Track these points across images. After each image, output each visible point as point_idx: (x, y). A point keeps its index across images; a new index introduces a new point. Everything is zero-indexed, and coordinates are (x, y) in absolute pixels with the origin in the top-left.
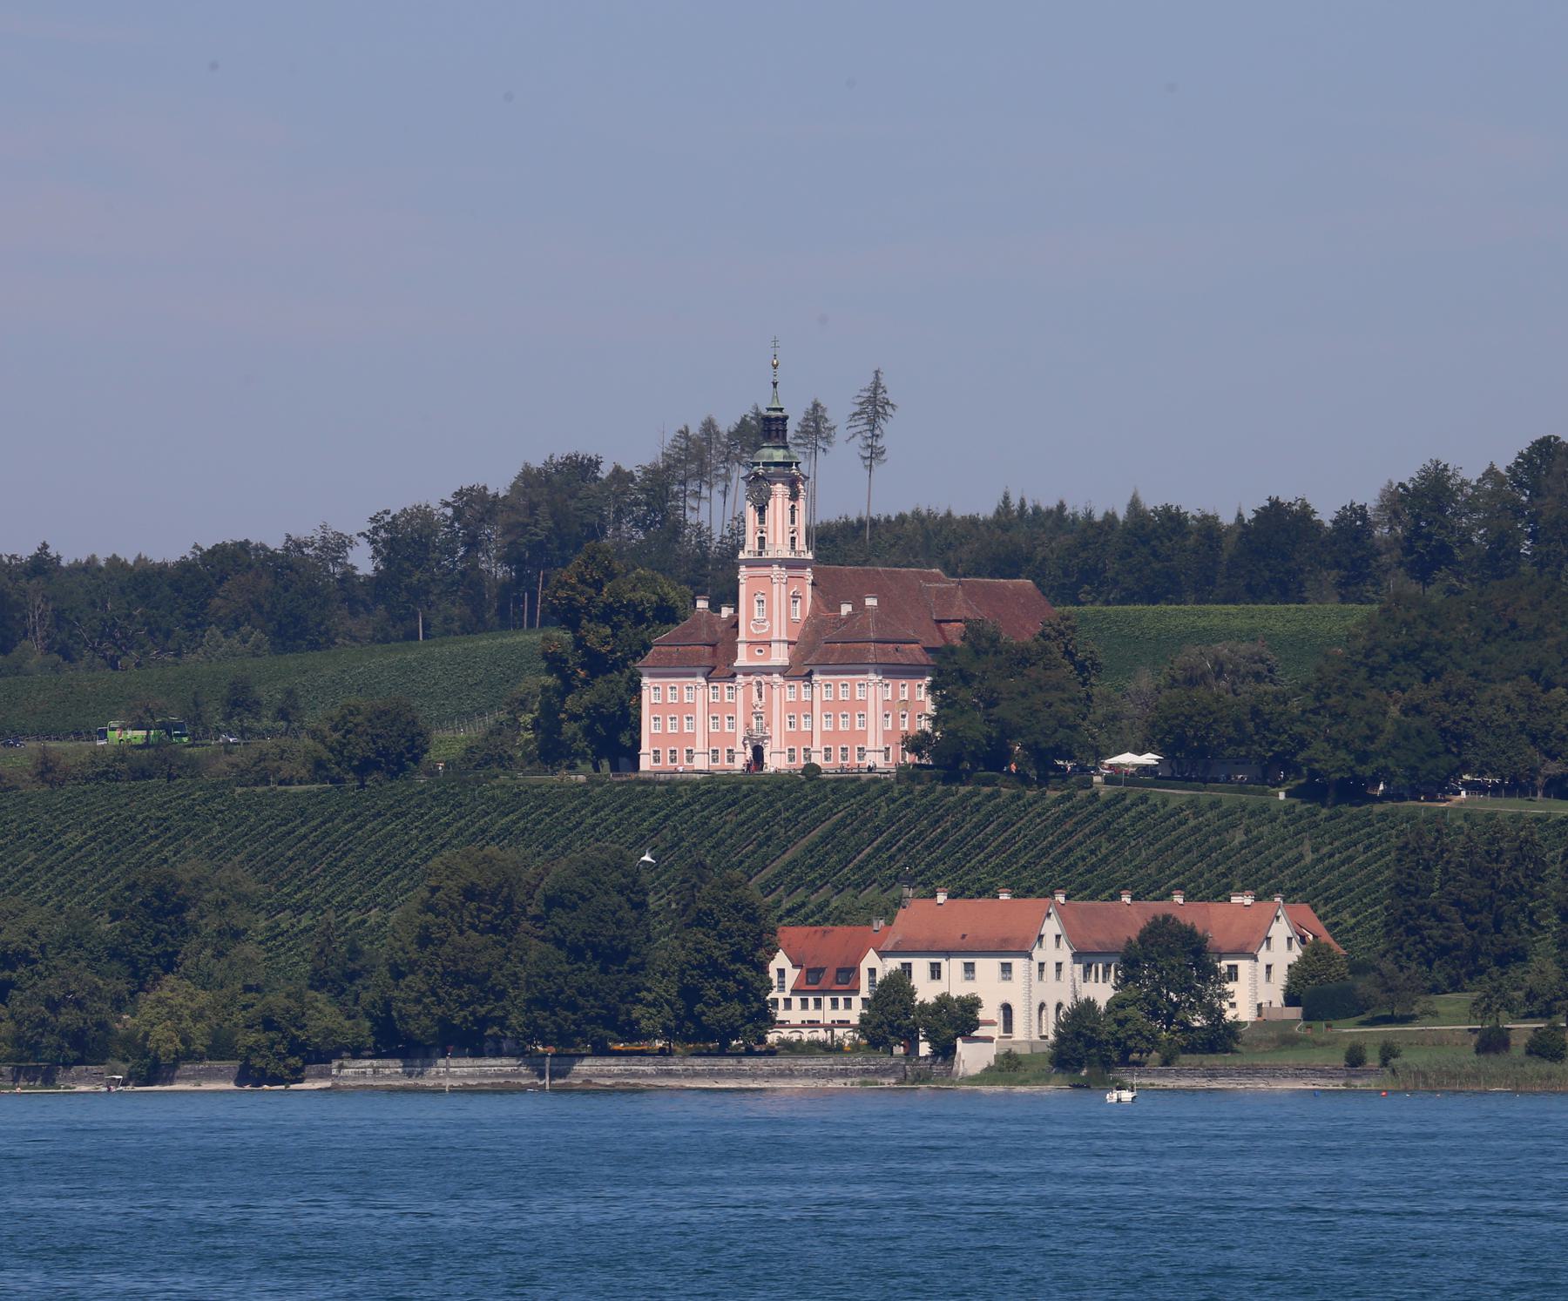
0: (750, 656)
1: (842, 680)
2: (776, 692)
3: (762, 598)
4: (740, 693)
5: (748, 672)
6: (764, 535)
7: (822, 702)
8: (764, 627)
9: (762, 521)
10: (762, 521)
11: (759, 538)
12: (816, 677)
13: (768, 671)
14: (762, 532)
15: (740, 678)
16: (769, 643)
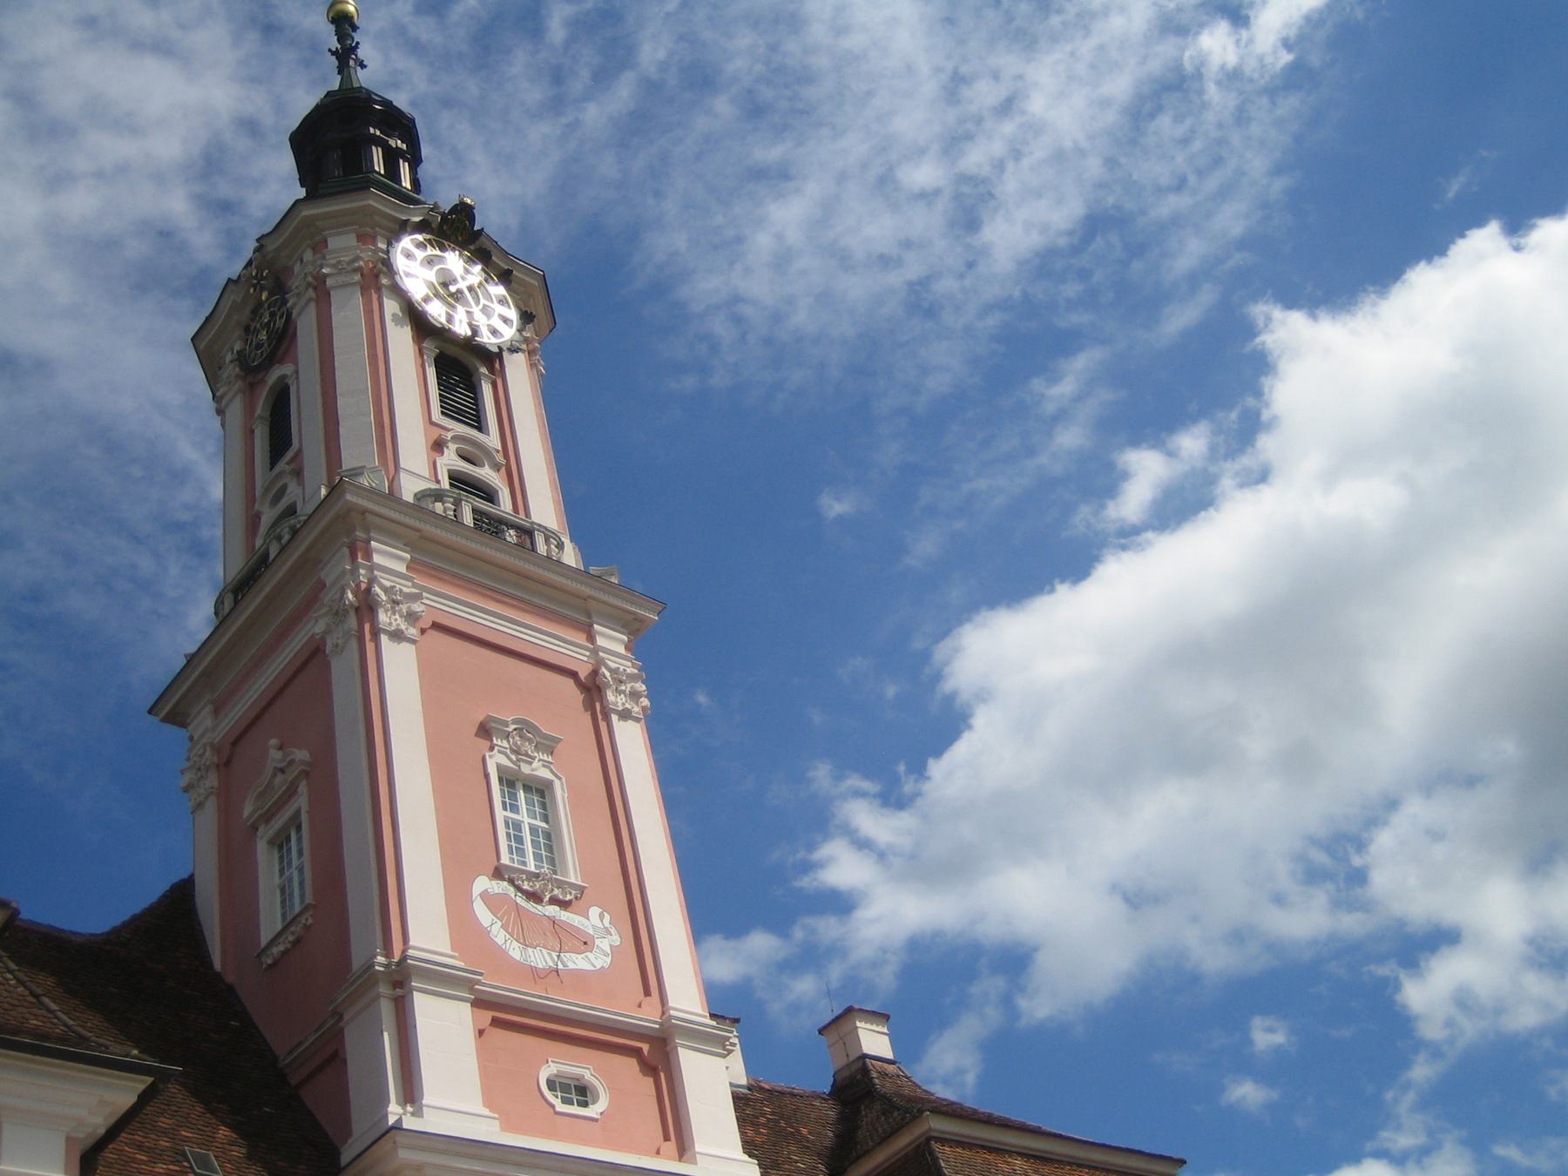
6: (486, 473)
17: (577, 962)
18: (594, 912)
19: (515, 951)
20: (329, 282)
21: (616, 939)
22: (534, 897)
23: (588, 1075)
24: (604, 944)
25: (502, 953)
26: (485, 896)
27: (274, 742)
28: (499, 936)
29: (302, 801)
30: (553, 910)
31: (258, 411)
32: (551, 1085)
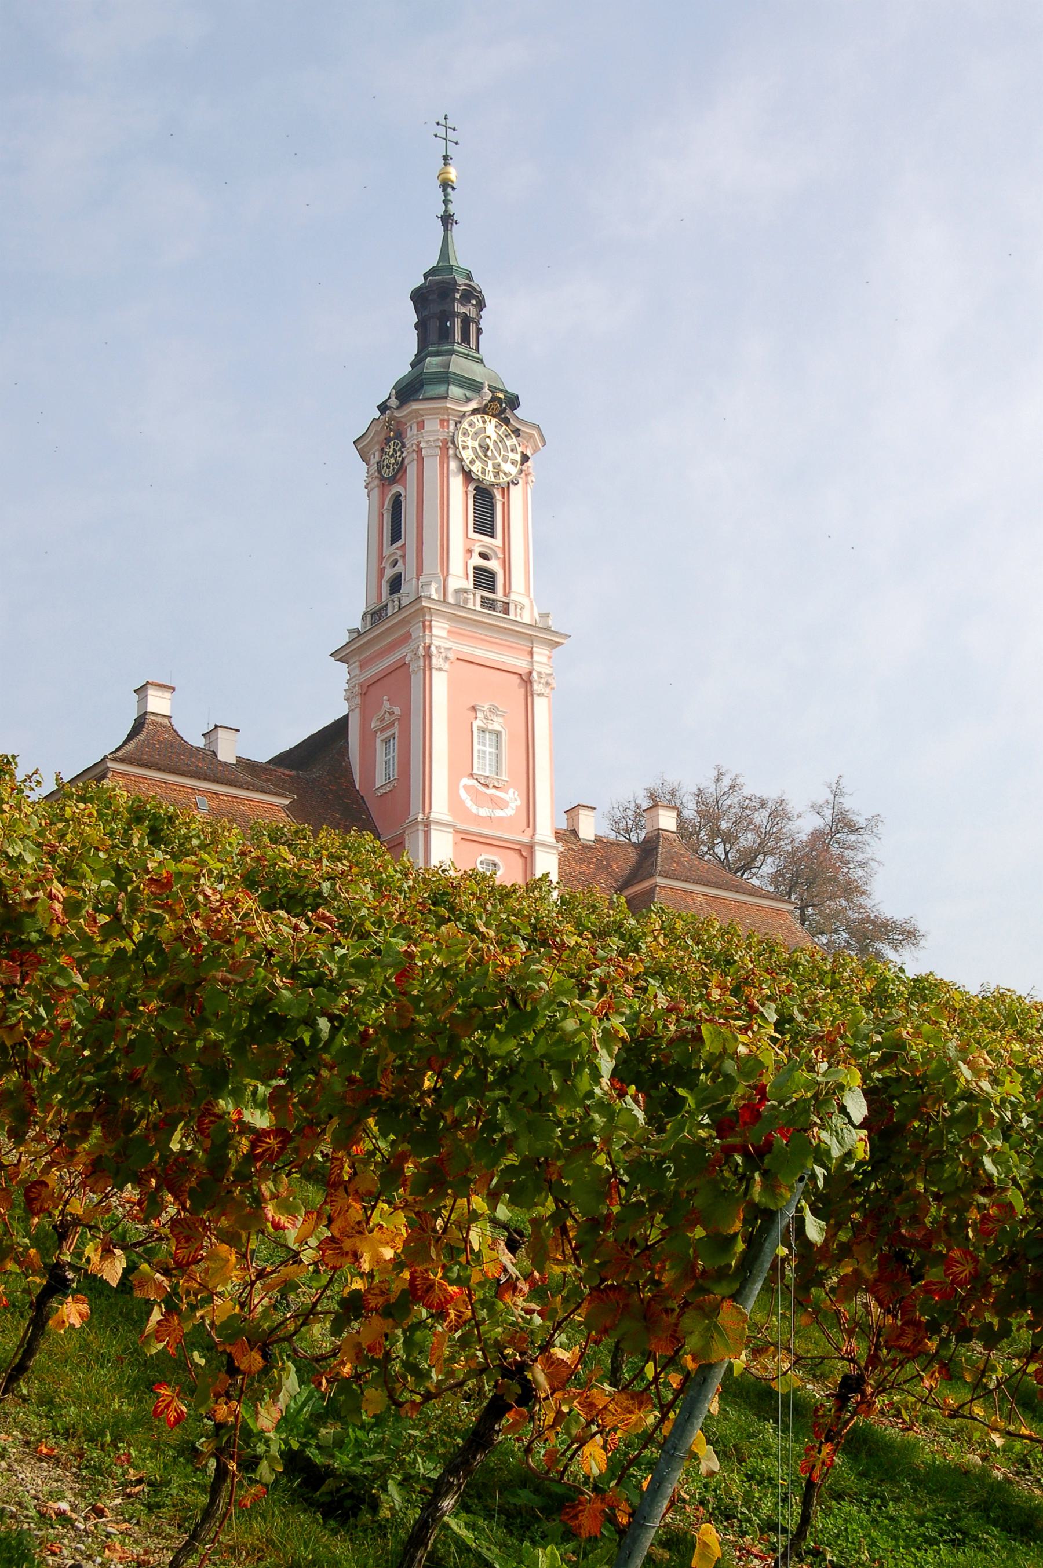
6: (494, 565)
9: (485, 524)
14: (484, 556)
16: (531, 847)
17: (499, 813)
18: (511, 791)
19: (474, 809)
20: (424, 452)
21: (519, 803)
22: (487, 786)
23: (497, 860)
24: (513, 805)
25: (470, 811)
26: (465, 787)
27: (385, 697)
28: (469, 803)
29: (395, 730)
30: (492, 791)
31: (386, 507)
32: (482, 863)
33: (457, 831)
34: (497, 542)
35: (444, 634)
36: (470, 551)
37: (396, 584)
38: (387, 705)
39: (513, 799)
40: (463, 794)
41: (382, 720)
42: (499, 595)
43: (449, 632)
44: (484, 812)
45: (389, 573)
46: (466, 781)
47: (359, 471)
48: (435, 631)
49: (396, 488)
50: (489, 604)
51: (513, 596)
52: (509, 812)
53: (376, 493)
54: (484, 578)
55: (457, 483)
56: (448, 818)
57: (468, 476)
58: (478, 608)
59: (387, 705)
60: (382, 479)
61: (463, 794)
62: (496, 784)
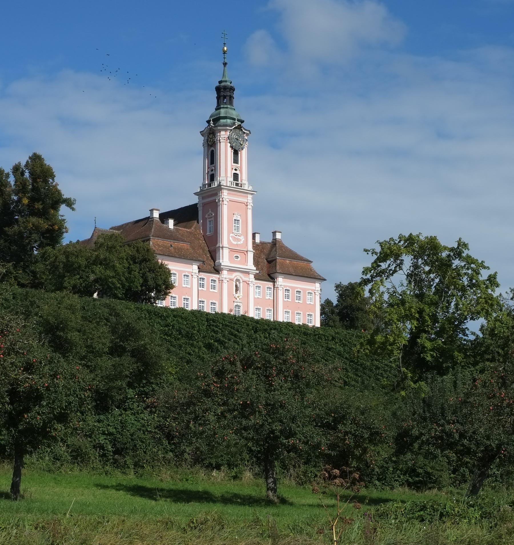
0: (231, 260)
1: (297, 288)
2: (251, 289)
3: (239, 218)
4: (225, 286)
5: (231, 270)
7: (284, 301)
8: (240, 240)
9: (236, 161)
10: (236, 161)
11: (234, 174)
12: (280, 281)
13: (247, 273)
14: (236, 170)
15: (225, 273)
16: (247, 252)
17: (239, 243)
20: (221, 141)
23: (239, 256)
24: (242, 240)
28: (232, 241)
33: (229, 248)
34: (239, 165)
35: (226, 195)
36: (232, 169)
37: (212, 178)
38: (210, 211)
39: (242, 238)
40: (230, 237)
41: (209, 215)
42: (239, 182)
43: (228, 193)
44: (235, 243)
45: (211, 173)
46: (231, 235)
47: (201, 139)
48: (224, 194)
49: (212, 148)
50: (237, 184)
51: (243, 182)
52: (242, 242)
53: (206, 148)
54: (236, 177)
55: (229, 149)
56: (227, 246)
57: (232, 147)
58: (235, 186)
59: (210, 211)
60: (208, 145)
61: (230, 237)
62: (239, 235)
